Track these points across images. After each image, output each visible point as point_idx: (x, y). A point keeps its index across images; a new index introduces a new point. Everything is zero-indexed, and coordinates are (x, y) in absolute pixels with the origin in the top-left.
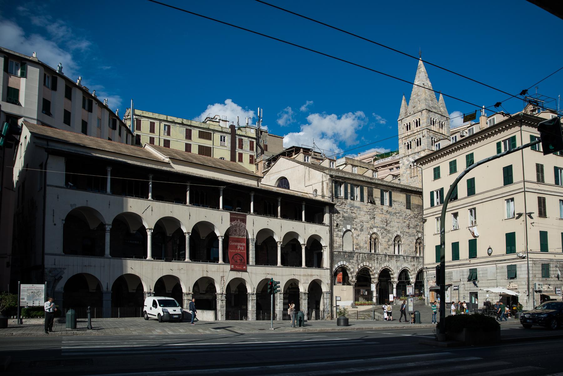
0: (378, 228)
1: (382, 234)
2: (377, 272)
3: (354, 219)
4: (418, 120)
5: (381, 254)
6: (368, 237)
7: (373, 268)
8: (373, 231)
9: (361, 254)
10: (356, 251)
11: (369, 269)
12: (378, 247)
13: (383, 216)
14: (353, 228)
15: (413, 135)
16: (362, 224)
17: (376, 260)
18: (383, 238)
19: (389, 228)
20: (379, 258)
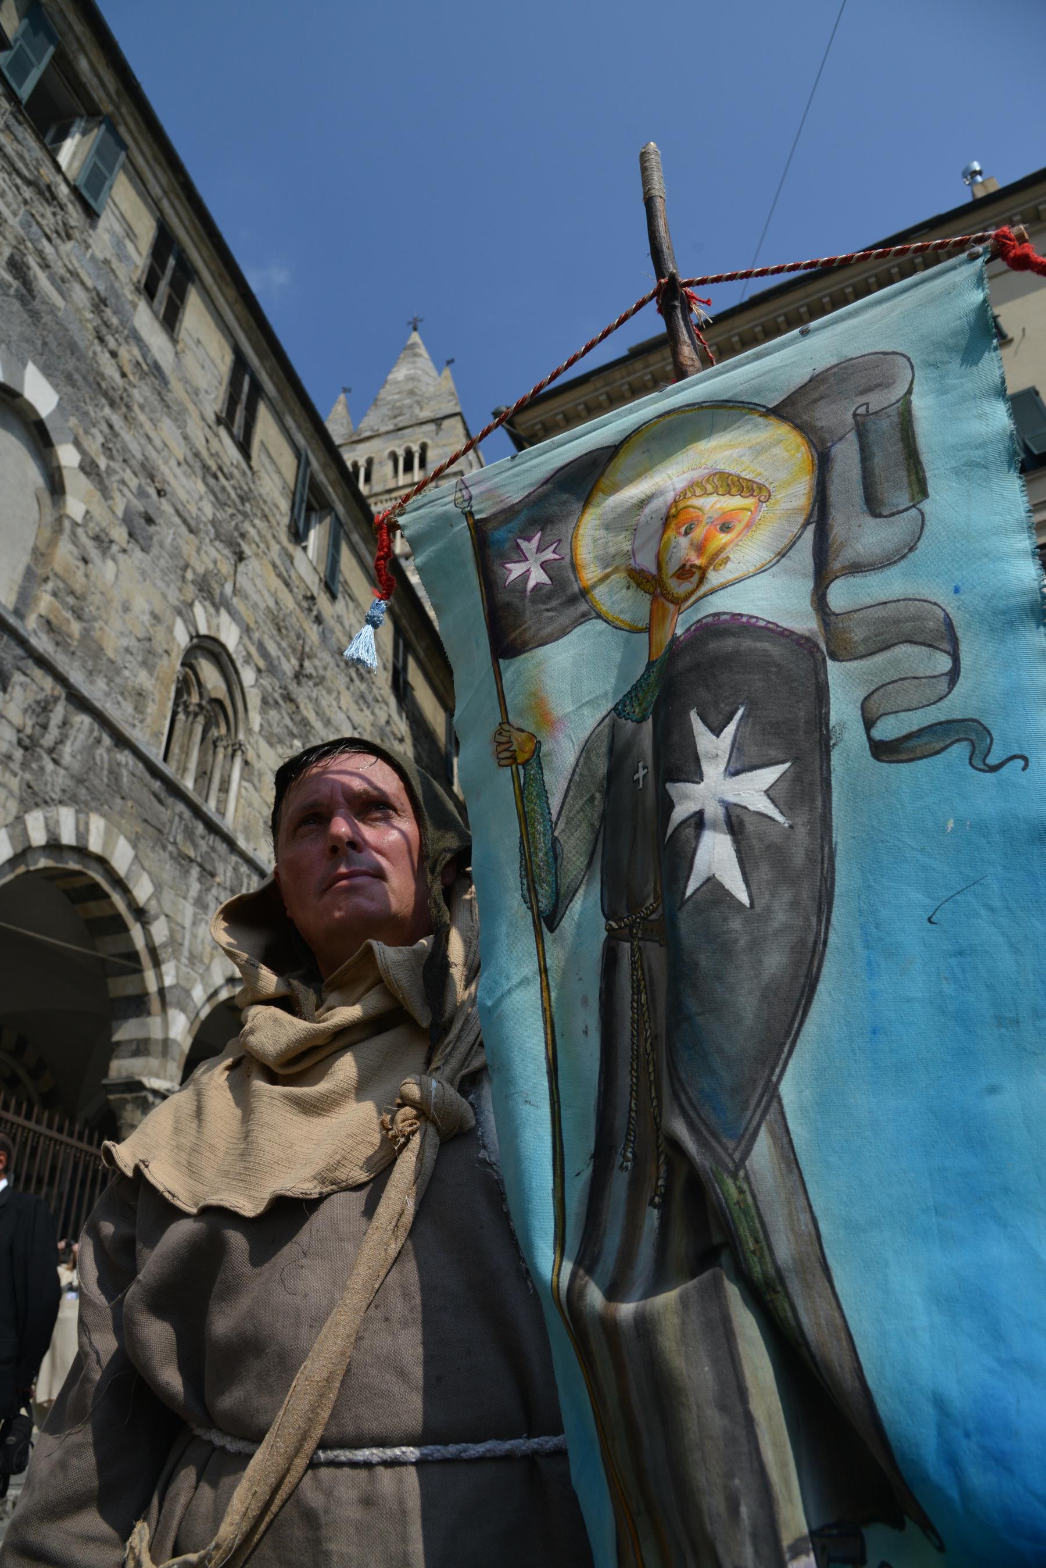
0: (246, 640)
1: (265, 701)
2: (188, 993)
3: (106, 395)
4: (416, 448)
5: (242, 843)
6: (170, 630)
7: (160, 931)
8: (214, 621)
9: (83, 721)
10: (42, 643)
11: (118, 925)
12: (224, 788)
13: (289, 602)
14: (77, 444)
15: (386, 497)
16: (152, 491)
17: (195, 871)
18: (271, 745)
19: (310, 706)
20: (220, 867)
